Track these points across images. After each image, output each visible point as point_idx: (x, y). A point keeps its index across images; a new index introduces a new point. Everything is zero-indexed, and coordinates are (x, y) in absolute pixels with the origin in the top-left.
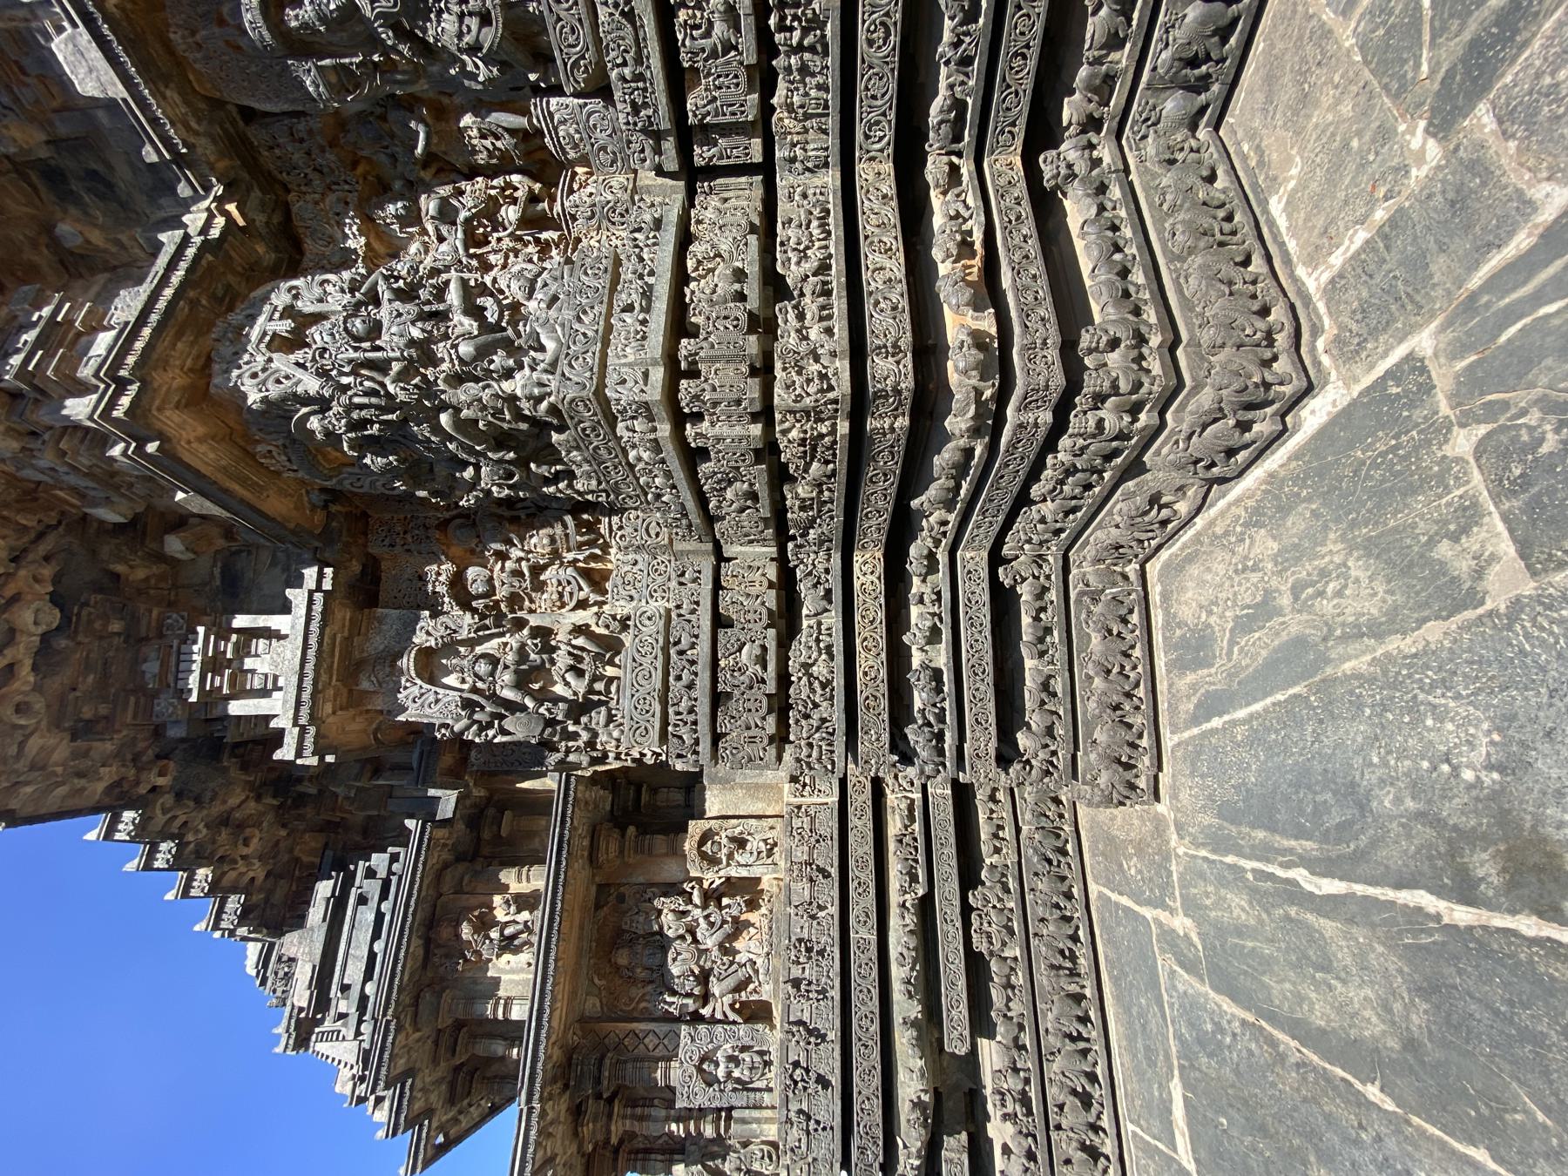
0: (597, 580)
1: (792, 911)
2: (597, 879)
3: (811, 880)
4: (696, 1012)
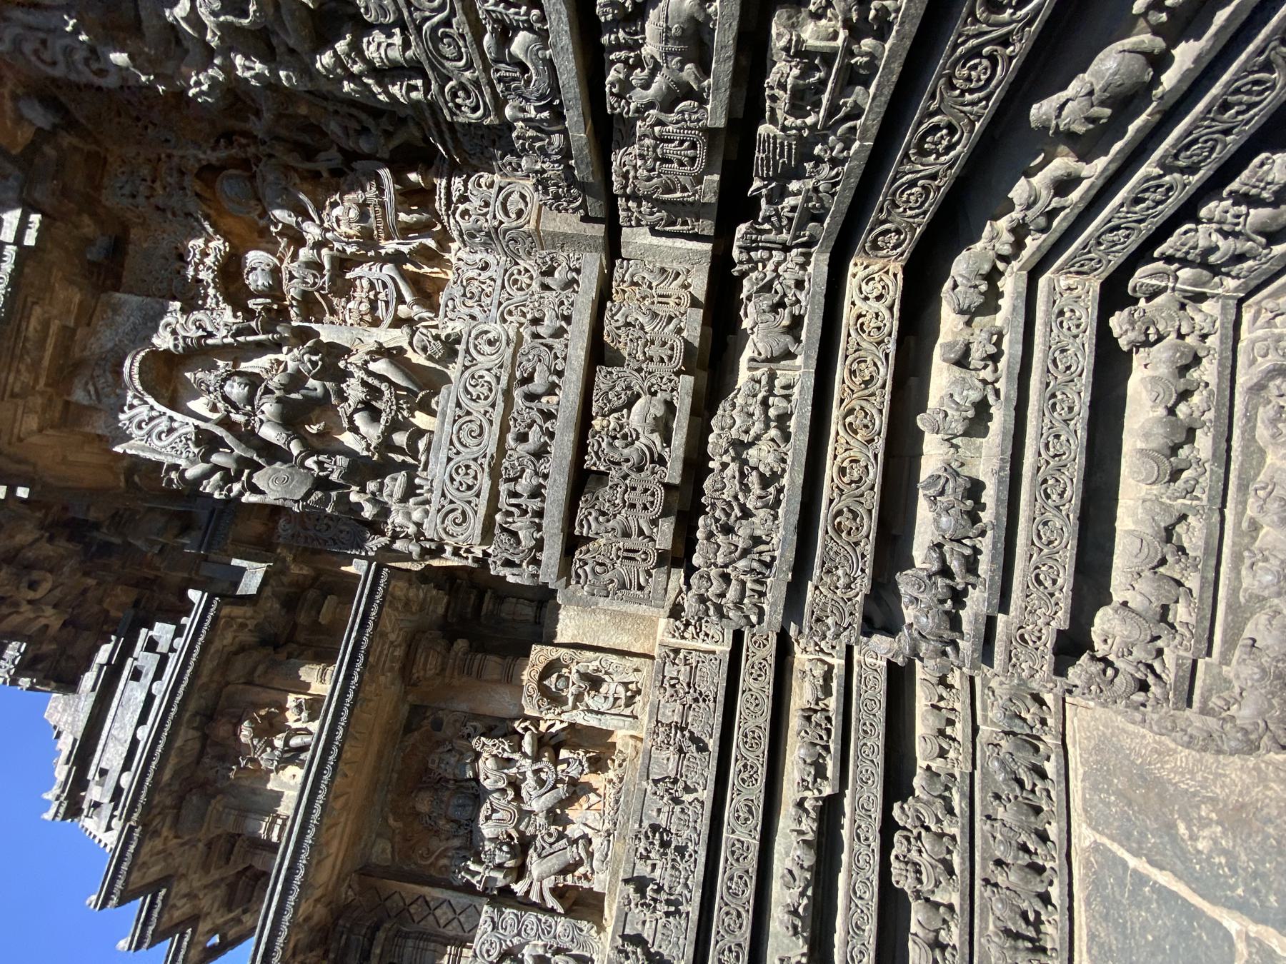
0: (427, 293)
1: (650, 787)
2: (410, 698)
3: (680, 750)
4: (508, 887)
